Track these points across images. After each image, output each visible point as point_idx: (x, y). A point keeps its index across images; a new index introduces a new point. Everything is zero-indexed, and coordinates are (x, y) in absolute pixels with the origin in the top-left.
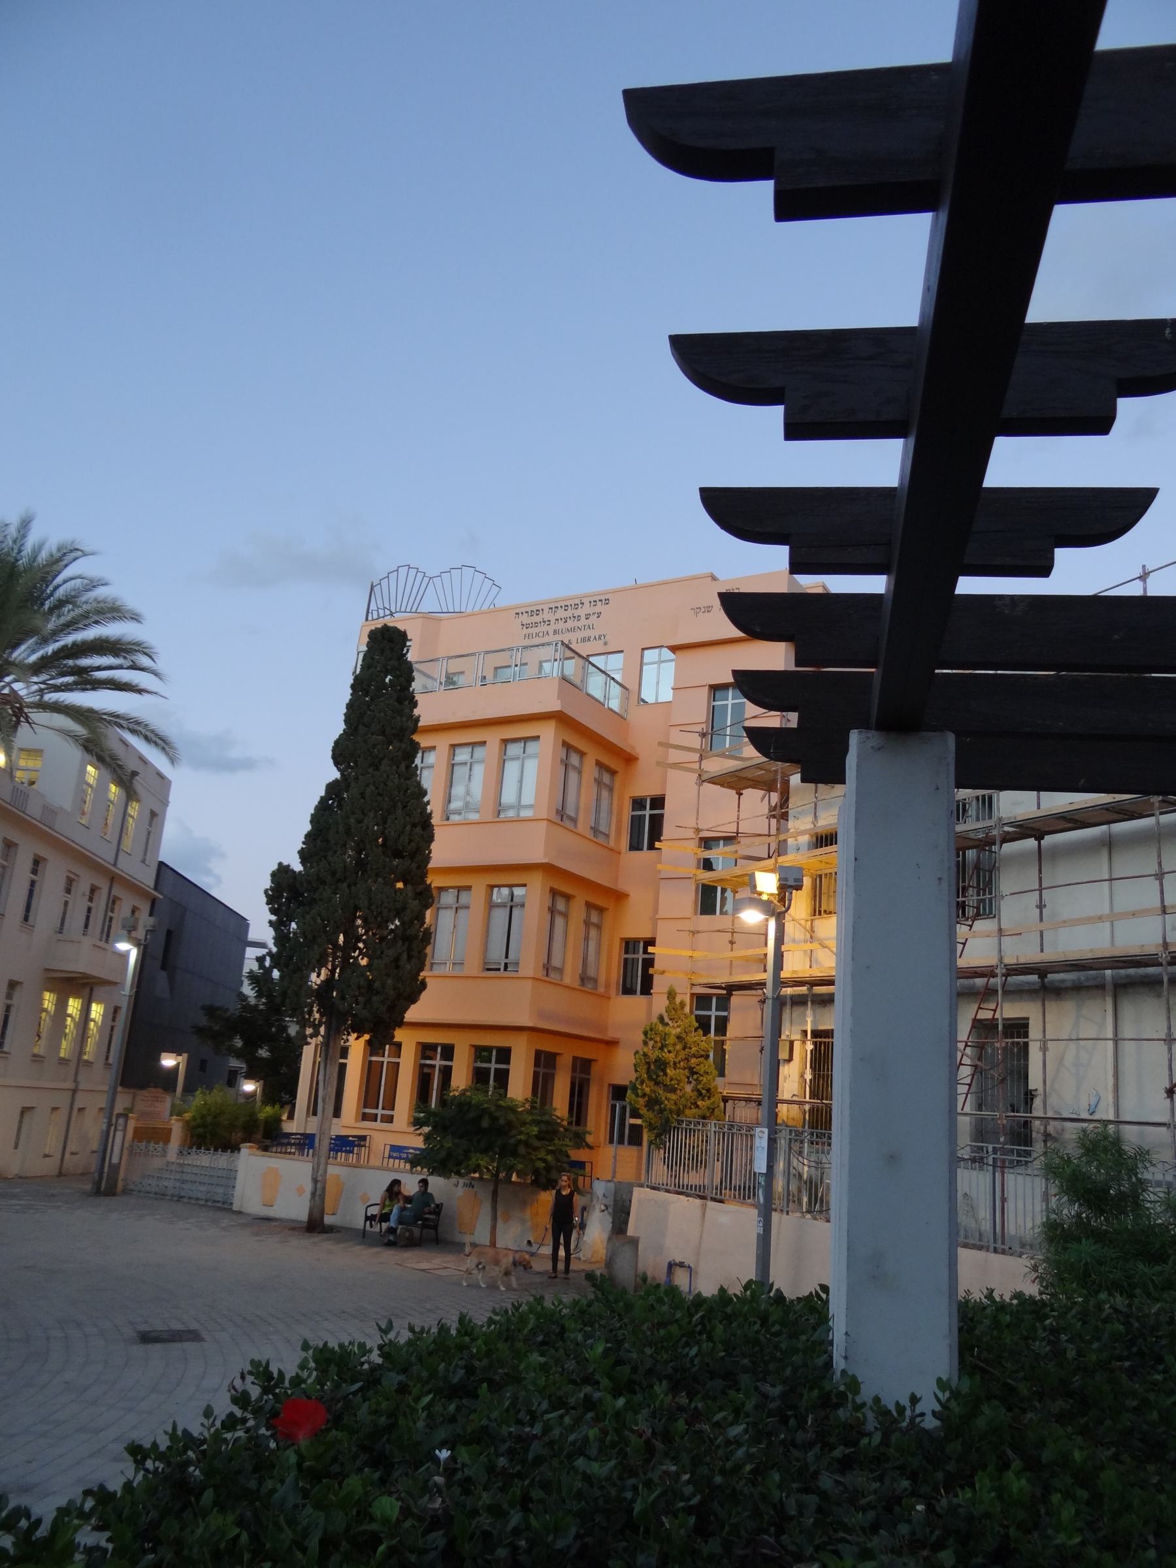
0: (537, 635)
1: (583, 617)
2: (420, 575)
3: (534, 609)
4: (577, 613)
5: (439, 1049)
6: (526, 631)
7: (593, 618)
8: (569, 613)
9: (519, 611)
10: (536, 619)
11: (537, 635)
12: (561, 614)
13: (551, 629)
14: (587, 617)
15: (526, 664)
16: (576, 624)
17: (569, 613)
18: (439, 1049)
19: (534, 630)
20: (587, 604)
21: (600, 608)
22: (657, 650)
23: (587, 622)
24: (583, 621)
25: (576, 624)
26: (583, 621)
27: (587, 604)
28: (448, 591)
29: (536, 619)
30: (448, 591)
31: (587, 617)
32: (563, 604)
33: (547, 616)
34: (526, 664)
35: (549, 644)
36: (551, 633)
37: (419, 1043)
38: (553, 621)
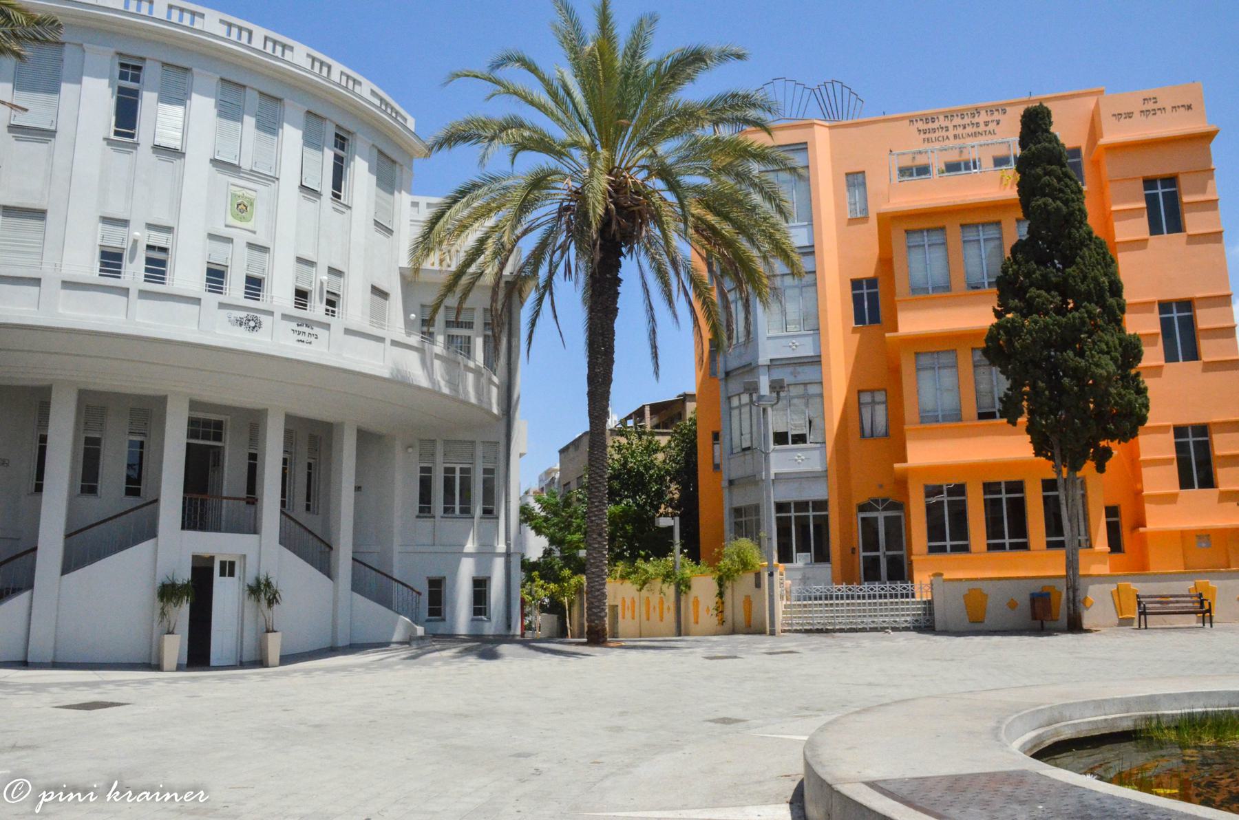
0: (937, 139)
1: (982, 125)
2: (800, 88)
6: (922, 136)
7: (992, 126)
8: (967, 121)
10: (931, 125)
13: (951, 133)
14: (986, 124)
16: (975, 129)
17: (967, 121)
19: (933, 136)
21: (996, 116)
23: (987, 129)
24: (982, 128)
25: (975, 129)
26: (982, 128)
27: (983, 112)
28: (832, 98)
29: (931, 125)
30: (832, 98)
31: (986, 124)
36: (951, 137)
38: (951, 128)
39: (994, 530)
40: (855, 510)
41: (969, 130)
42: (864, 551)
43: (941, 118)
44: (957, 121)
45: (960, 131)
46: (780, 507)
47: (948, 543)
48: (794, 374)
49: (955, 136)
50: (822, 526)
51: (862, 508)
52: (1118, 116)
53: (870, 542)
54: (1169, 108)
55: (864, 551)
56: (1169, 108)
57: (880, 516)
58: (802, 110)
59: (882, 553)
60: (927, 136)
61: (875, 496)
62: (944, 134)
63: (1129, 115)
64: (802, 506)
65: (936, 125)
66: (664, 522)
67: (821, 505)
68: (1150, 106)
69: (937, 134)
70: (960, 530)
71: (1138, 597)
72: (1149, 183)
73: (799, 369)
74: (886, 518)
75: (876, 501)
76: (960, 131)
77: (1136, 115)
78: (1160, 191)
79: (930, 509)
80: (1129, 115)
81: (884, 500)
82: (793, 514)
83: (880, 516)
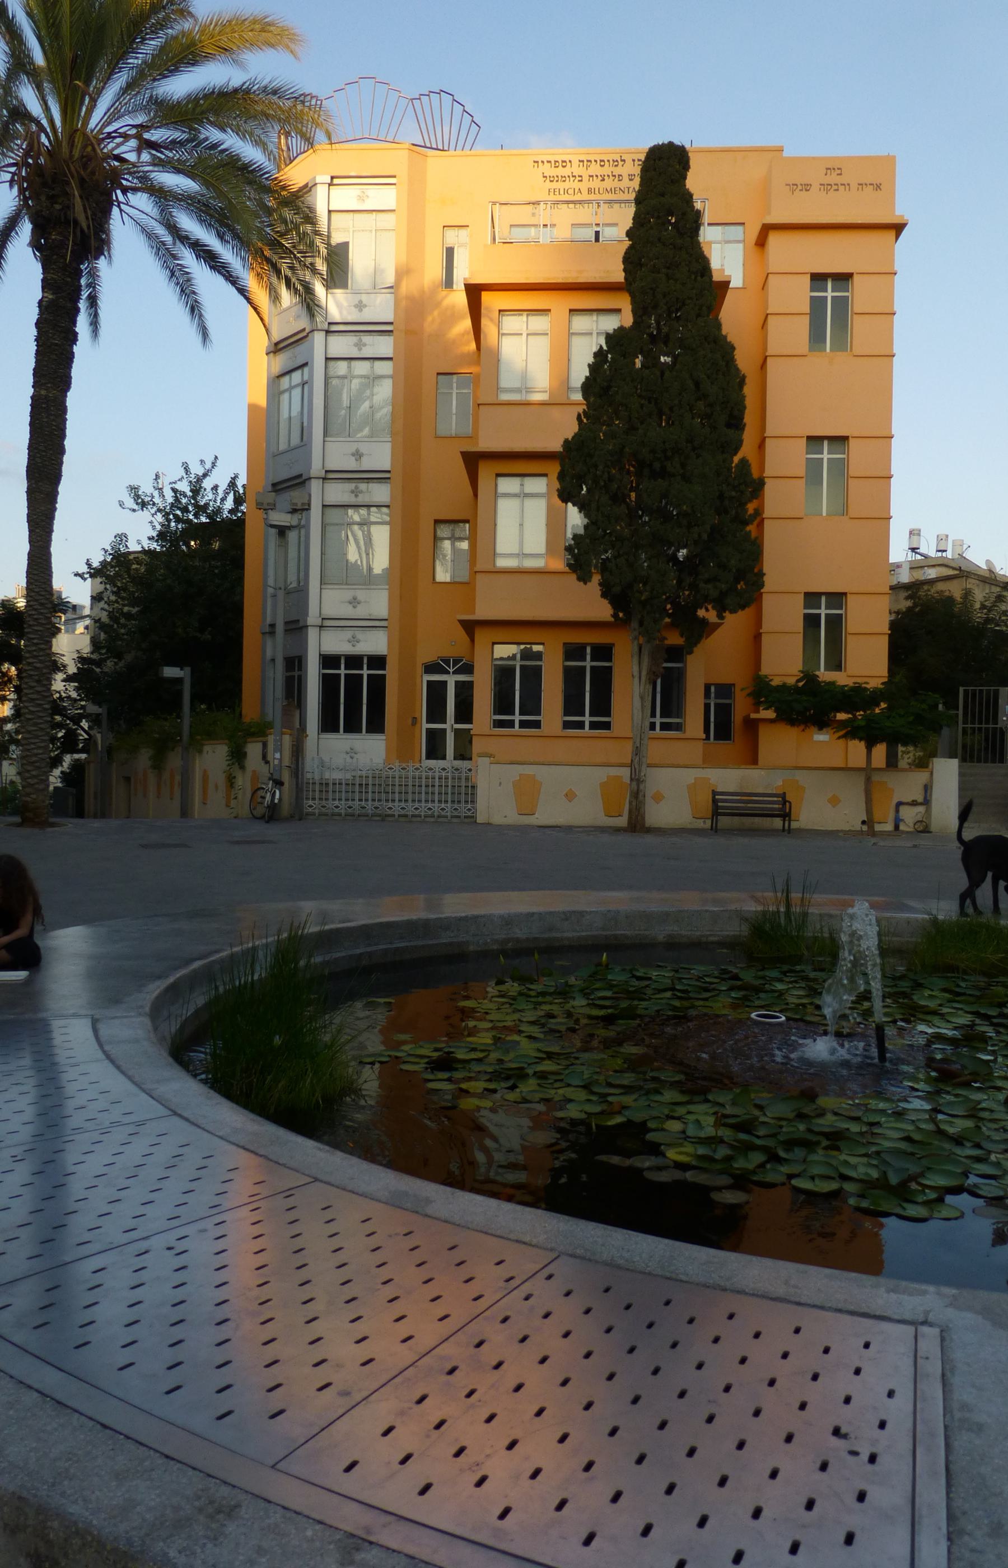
0: (566, 192)
1: (626, 179)
3: (560, 158)
4: (617, 171)
5: (589, 650)
9: (539, 159)
10: (560, 171)
11: (566, 192)
12: (595, 169)
13: (584, 186)
15: (553, 225)
16: (616, 184)
17: (607, 170)
18: (589, 650)
19: (561, 185)
20: (629, 162)
22: (719, 228)
25: (616, 184)
29: (560, 171)
32: (598, 158)
33: (577, 169)
34: (553, 225)
35: (589, 202)
36: (585, 191)
37: (564, 644)
38: (585, 178)
39: (572, 704)
40: (420, 669)
41: (609, 183)
42: (428, 722)
43: (576, 163)
44: (595, 169)
45: (596, 184)
46: (329, 661)
47: (517, 718)
48: (356, 492)
49: (590, 191)
50: (378, 685)
51: (431, 668)
52: (793, 187)
53: (436, 712)
54: (854, 186)
55: (428, 722)
56: (854, 186)
57: (451, 680)
58: (393, 130)
59: (450, 725)
60: (555, 185)
61: (446, 653)
62: (576, 185)
63: (807, 187)
64: (354, 661)
65: (566, 172)
66: (170, 672)
67: (378, 661)
68: (833, 178)
69: (567, 185)
70: (532, 704)
71: (714, 793)
72: (818, 279)
73: (363, 486)
74: (456, 682)
75: (447, 661)
76: (596, 184)
77: (815, 187)
78: (829, 294)
79: (567, 671)
80: (807, 187)
81: (456, 662)
82: (342, 671)
83: (451, 680)
